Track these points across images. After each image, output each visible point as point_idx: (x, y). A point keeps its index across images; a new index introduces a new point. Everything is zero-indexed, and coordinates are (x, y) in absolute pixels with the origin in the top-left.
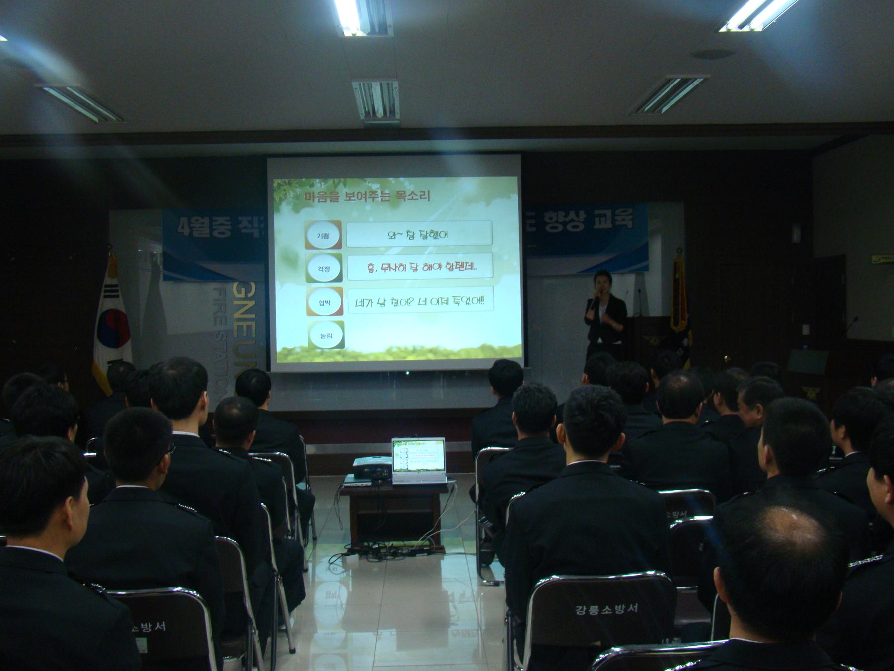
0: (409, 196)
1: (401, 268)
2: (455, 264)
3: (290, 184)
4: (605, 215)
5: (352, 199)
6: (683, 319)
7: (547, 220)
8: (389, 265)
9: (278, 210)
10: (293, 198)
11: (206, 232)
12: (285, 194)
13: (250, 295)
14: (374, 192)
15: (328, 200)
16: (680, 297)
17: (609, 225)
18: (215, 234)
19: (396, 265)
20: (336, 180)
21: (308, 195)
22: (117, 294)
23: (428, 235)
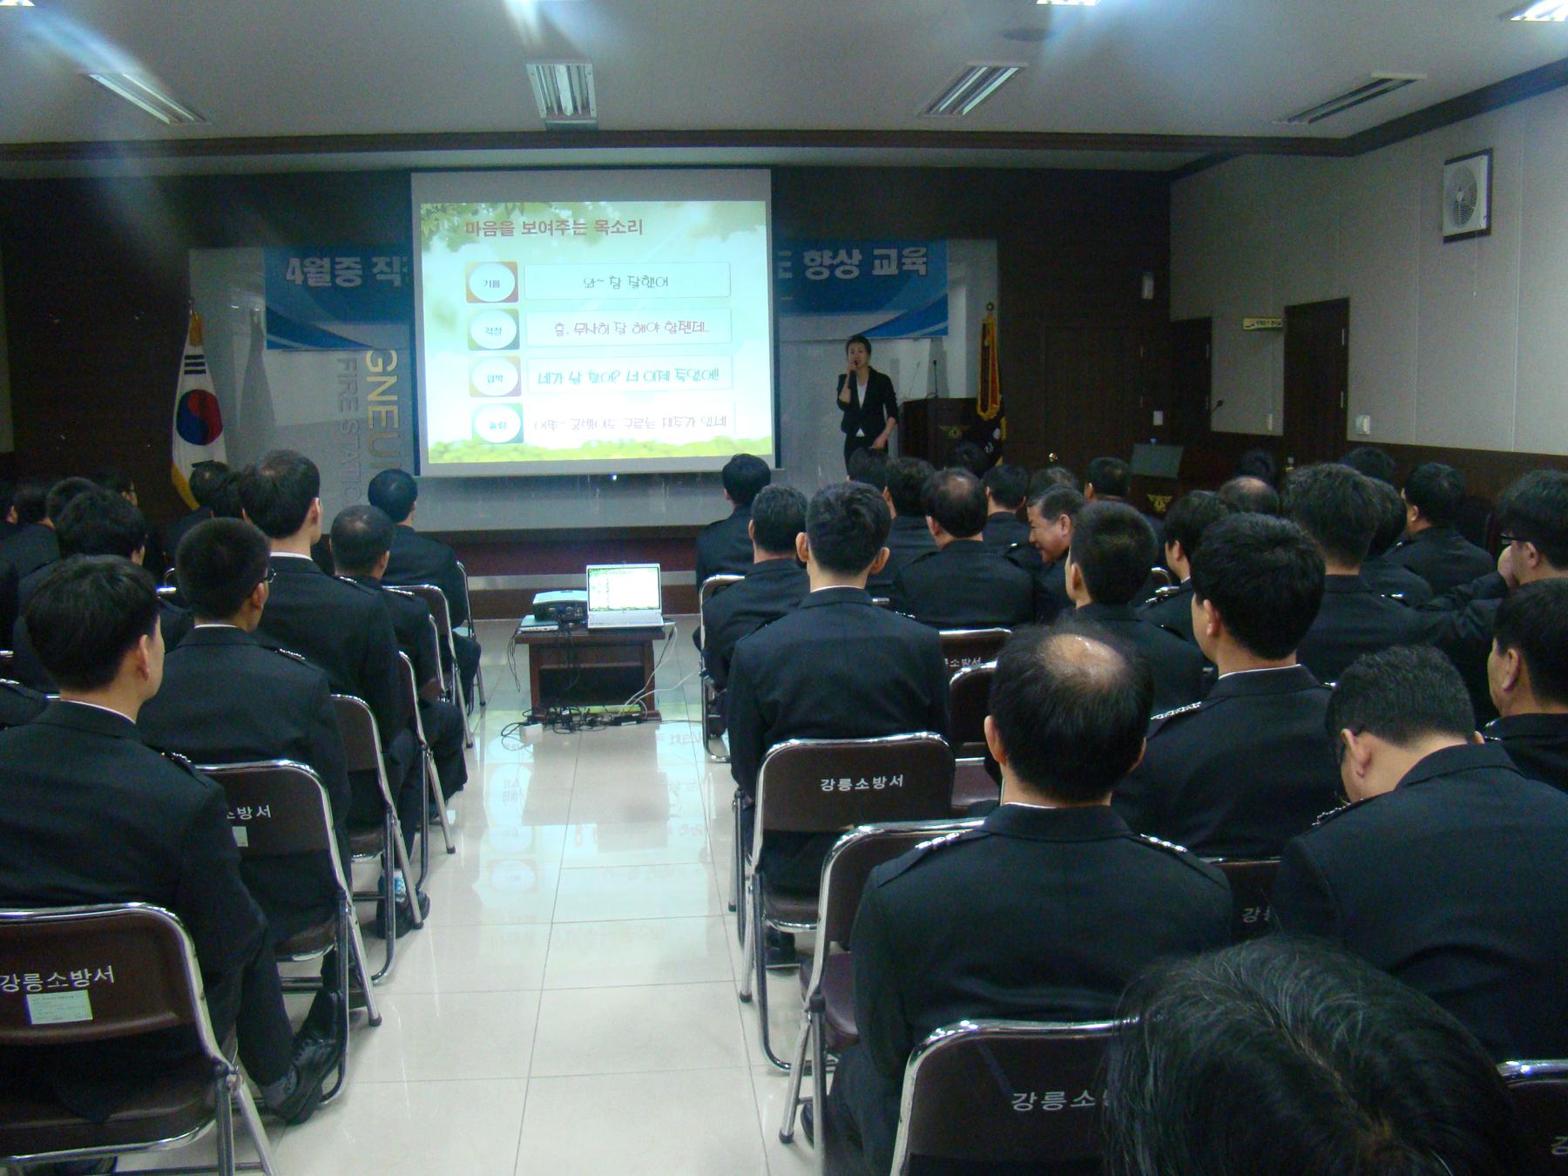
0: (613, 227)
1: (603, 329)
2: (678, 324)
3: (444, 210)
5: (532, 231)
6: (994, 402)
7: (807, 261)
8: (585, 325)
9: (428, 248)
11: (326, 280)
12: (438, 226)
13: (390, 368)
14: (564, 222)
15: (499, 233)
16: (990, 368)
17: (892, 270)
18: (339, 281)
20: (510, 205)
21: (470, 227)
22: (199, 368)
23: (640, 283)
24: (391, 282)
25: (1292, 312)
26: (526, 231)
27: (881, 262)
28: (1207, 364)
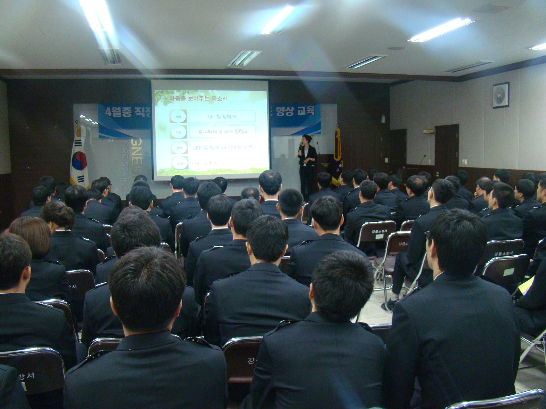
0: (218, 99)
1: (215, 132)
2: (239, 130)
3: (162, 92)
4: (302, 109)
5: (192, 99)
6: (340, 155)
7: (277, 110)
8: (209, 130)
9: (157, 105)
10: (164, 99)
12: (160, 97)
13: (139, 144)
14: (202, 97)
15: (180, 100)
17: (304, 113)
18: (124, 115)
19: (212, 131)
20: (184, 91)
21: (171, 98)
23: (227, 117)
24: (141, 116)
25: (437, 128)
26: (190, 99)
27: (300, 111)
28: (405, 144)
